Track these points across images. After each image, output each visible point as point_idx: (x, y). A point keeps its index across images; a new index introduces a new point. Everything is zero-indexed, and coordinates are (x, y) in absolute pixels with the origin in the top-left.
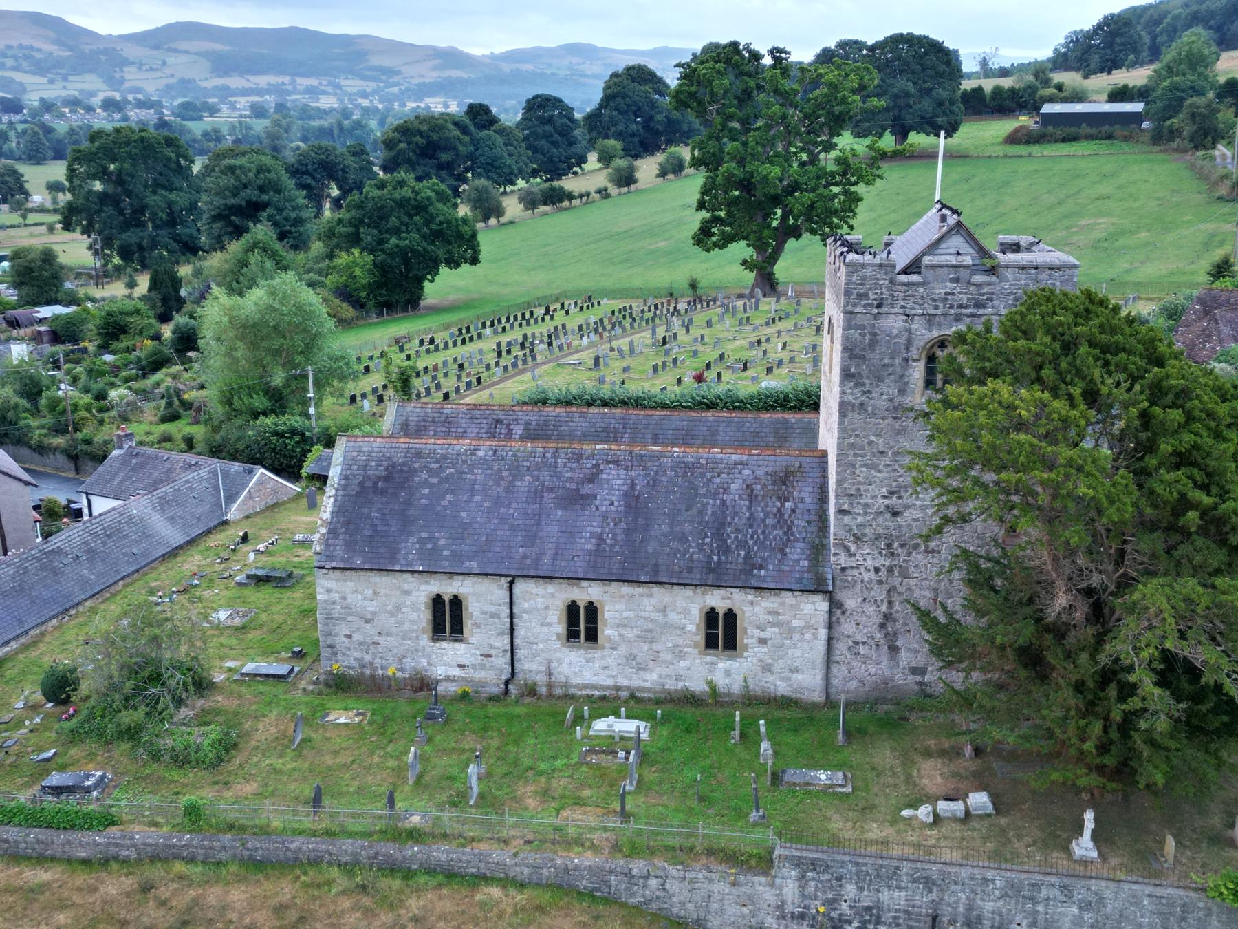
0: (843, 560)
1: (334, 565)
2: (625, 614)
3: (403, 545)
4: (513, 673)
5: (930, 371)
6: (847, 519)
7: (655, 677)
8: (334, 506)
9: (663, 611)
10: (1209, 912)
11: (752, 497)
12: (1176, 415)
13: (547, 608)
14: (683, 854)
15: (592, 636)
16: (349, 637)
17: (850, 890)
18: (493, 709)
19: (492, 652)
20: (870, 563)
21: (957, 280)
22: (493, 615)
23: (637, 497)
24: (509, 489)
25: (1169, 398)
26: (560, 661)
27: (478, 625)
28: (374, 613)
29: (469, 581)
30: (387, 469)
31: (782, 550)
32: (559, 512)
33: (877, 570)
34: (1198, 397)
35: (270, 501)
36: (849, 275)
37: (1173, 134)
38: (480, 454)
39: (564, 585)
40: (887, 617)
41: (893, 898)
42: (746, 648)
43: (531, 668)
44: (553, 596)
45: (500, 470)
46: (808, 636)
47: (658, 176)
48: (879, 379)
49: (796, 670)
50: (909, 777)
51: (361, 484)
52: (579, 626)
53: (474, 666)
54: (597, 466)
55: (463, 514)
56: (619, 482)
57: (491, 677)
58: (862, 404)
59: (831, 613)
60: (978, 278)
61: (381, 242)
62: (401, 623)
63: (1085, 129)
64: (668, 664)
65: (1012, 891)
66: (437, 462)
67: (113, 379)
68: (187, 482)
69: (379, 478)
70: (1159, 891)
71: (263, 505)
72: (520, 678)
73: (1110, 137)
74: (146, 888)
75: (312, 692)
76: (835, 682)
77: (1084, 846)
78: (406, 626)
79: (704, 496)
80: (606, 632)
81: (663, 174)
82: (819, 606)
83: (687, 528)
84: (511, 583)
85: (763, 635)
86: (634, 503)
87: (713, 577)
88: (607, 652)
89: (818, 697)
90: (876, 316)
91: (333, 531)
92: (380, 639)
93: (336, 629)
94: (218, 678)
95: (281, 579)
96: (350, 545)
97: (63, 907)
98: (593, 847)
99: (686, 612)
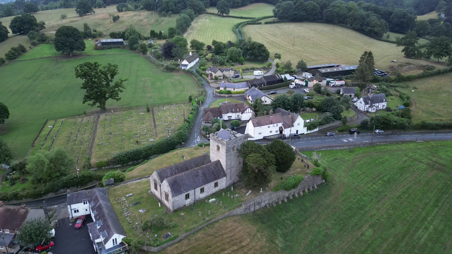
0: (227, 172)
9: (210, 185)
11: (215, 168)
14: (234, 208)
15: (203, 191)
17: (248, 204)
24: (189, 177)
37: (135, 49)
40: (231, 176)
41: (251, 203)
43: (197, 198)
49: (223, 186)
57: (193, 202)
60: (236, 139)
69: (173, 182)
72: (196, 200)
73: (119, 47)
74: (189, 240)
75: (173, 213)
80: (205, 190)
82: (225, 177)
86: (204, 174)
87: (216, 179)
89: (225, 188)
96: (175, 192)
97: (182, 246)
98: (227, 212)
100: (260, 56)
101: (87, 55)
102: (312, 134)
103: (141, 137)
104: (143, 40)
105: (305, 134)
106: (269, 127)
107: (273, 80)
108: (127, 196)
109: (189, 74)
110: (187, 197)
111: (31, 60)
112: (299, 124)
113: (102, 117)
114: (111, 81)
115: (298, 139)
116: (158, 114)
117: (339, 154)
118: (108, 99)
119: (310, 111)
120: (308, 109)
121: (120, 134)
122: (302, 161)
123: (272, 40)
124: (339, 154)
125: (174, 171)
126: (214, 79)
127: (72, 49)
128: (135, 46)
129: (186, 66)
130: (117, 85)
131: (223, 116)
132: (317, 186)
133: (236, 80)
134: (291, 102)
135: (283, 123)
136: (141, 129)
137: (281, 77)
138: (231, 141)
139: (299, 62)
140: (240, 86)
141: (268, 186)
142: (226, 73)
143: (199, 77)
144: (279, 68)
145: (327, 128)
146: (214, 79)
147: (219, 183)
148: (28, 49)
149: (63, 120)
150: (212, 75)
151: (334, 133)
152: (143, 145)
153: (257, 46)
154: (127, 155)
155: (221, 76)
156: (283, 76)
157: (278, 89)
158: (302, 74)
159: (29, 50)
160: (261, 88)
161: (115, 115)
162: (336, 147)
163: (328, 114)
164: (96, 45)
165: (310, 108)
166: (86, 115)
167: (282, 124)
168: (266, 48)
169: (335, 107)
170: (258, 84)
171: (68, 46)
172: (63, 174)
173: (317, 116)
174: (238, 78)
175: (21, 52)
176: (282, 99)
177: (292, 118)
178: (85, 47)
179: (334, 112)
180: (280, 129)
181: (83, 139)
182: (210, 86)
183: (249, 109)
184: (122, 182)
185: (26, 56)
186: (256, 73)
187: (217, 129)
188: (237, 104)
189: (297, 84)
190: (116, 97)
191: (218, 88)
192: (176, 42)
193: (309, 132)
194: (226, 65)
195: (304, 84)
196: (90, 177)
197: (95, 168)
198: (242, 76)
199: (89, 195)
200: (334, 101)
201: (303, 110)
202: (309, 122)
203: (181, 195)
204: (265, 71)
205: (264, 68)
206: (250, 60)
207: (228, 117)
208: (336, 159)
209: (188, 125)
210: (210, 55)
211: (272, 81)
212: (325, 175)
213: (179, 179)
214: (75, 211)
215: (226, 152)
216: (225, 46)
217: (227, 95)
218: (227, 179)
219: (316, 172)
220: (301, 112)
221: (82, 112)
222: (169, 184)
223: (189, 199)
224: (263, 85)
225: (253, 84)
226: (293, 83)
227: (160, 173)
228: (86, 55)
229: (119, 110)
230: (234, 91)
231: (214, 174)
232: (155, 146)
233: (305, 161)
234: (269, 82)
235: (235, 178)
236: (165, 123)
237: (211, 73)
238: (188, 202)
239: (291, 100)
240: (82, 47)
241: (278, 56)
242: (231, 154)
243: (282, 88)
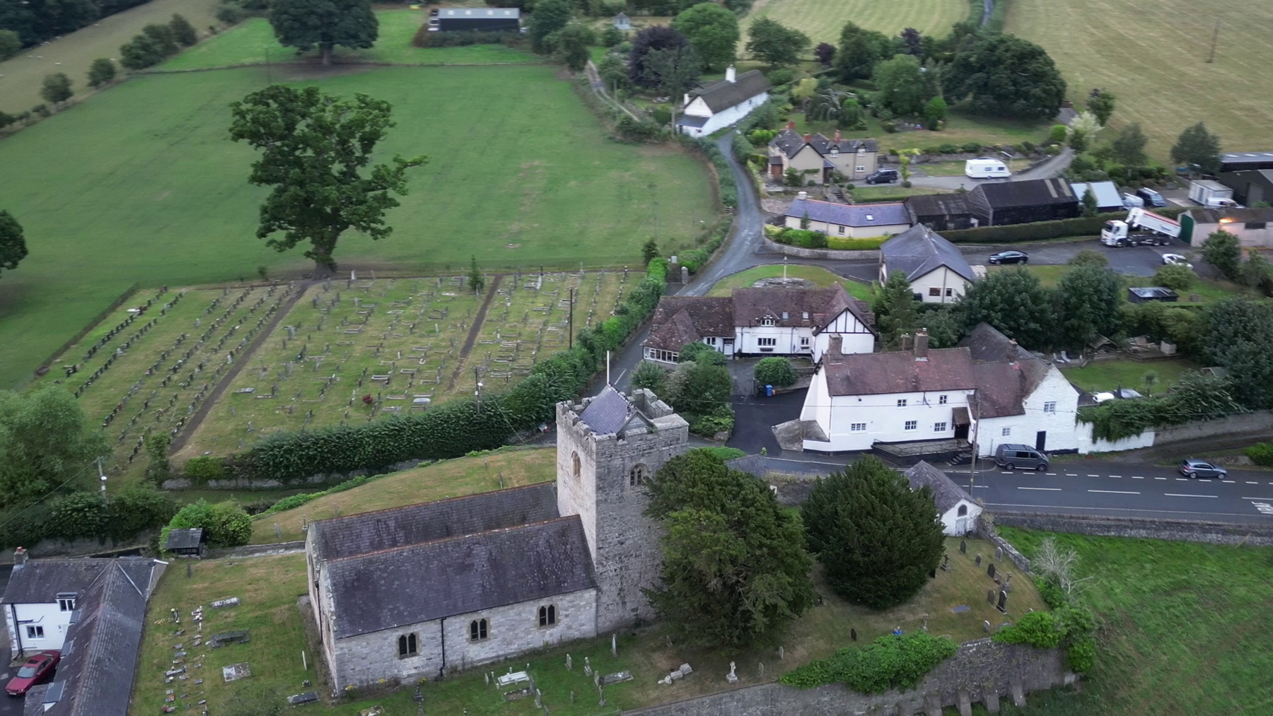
0: (601, 569)
1: (347, 635)
2: (501, 620)
3: (381, 615)
4: (444, 664)
5: (632, 478)
6: (601, 551)
7: (516, 646)
8: (334, 602)
9: (519, 614)
10: (780, 689)
11: (550, 546)
12: (752, 510)
13: (461, 627)
15: (484, 635)
18: (443, 686)
19: (432, 656)
20: (612, 568)
21: (641, 440)
22: (432, 638)
23: (495, 560)
25: (748, 503)
26: (468, 652)
27: (424, 645)
28: (367, 654)
29: (419, 625)
30: (356, 574)
31: (572, 571)
32: (458, 577)
33: (615, 570)
34: (758, 500)
36: (597, 446)
38: (405, 554)
39: (470, 614)
40: (621, 590)
42: (559, 621)
43: (454, 658)
44: (464, 621)
45: (419, 561)
46: (587, 608)
47: (90, 85)
48: (612, 487)
49: (583, 625)
50: (652, 664)
51: (344, 586)
52: (477, 631)
53: (422, 666)
54: (469, 547)
55: (408, 590)
56: (483, 553)
57: (432, 670)
58: (606, 500)
59: (597, 595)
60: (650, 437)
62: (383, 655)
63: (478, 34)
64: (522, 638)
65: (713, 704)
66: (383, 564)
69: (353, 580)
70: (763, 687)
72: (448, 665)
73: (498, 41)
75: (339, 703)
76: (599, 625)
77: (732, 677)
79: (528, 551)
80: (492, 631)
81: (95, 83)
82: (593, 593)
84: (442, 621)
85: (567, 613)
86: (495, 563)
87: (544, 592)
88: (492, 640)
89: (594, 634)
90: (609, 461)
95: (241, 638)
96: (351, 622)
100: (1018, 95)
101: (378, 61)
102: (1117, 459)
103: (394, 386)
104: (596, 16)
105: (1081, 455)
106: (902, 403)
107: (1027, 204)
108: (217, 603)
109: (698, 154)
110: (408, 646)
111: (198, 71)
112: (1050, 407)
113: (314, 291)
114: (362, 161)
115: (1037, 470)
116: (502, 301)
117: (1211, 567)
118: (347, 227)
119: (1145, 356)
120: (1138, 343)
121: (330, 364)
122: (991, 571)
123: (1121, 31)
124: (1211, 567)
125: (389, 534)
126: (785, 181)
127: (328, 41)
128: (551, 37)
129: (700, 121)
130: (382, 180)
131: (739, 335)
132: (1027, 695)
133: (876, 191)
134: (1045, 305)
135: (972, 392)
136: (413, 352)
137: (1068, 194)
138: (620, 442)
139: (1188, 131)
140: (870, 217)
141: (779, 658)
142: (839, 161)
143: (736, 174)
144: (1085, 153)
145: (1200, 438)
146: (785, 181)
147: (563, 613)
148: (202, 32)
149: (184, 290)
150: (781, 165)
151: (1220, 465)
152: (385, 413)
153: (1008, 54)
154: (301, 445)
155: (816, 171)
156: (1080, 189)
157: (1044, 243)
158: (1188, 187)
159: (206, 36)
160: (962, 231)
161: (358, 289)
162: (1205, 530)
163: (1215, 376)
164: (425, 27)
165: (1149, 341)
166: (267, 280)
167: (968, 396)
168: (1051, 63)
169: (1247, 346)
170: (952, 216)
171: (316, 28)
172: (56, 485)
173: (1156, 380)
174: (888, 182)
175: (178, 45)
176: (1004, 286)
177: (1022, 377)
178: (374, 36)
179: (1241, 370)
180: (954, 420)
181: (201, 367)
182: (760, 208)
183: (851, 318)
184: (238, 549)
185: (191, 58)
186: (978, 167)
187: (686, 385)
188: (804, 293)
189: (1139, 226)
190: (373, 225)
191: (780, 220)
192: (692, 28)
193: (1103, 446)
194: (864, 129)
195: (1173, 230)
196: (145, 511)
197: (182, 480)
198: (906, 177)
199: (87, 579)
200: (1250, 320)
201: (1110, 348)
202: (1106, 402)
203: (378, 635)
204: (1024, 164)
205: (1024, 148)
206: (974, 114)
207: (760, 340)
208: (1186, 586)
209: (582, 359)
210: (807, 85)
211: (1024, 208)
212: (1074, 651)
213: (384, 571)
214: (32, 632)
215: (599, 488)
216: (887, 50)
217: (806, 252)
218: (604, 599)
219: (1027, 632)
220: (1101, 356)
221: (254, 269)
222: (334, 585)
223: (415, 659)
224: (974, 221)
225: (926, 214)
226: (1118, 223)
227: (329, 536)
228: (375, 64)
230: (840, 236)
231: (541, 570)
232: (418, 424)
233: (1003, 571)
234: (1008, 210)
235: (638, 604)
236: (509, 338)
237: (779, 158)
238: (410, 668)
239: (1047, 297)
240: (365, 34)
241: (1102, 106)
242: (621, 498)
243: (1069, 239)
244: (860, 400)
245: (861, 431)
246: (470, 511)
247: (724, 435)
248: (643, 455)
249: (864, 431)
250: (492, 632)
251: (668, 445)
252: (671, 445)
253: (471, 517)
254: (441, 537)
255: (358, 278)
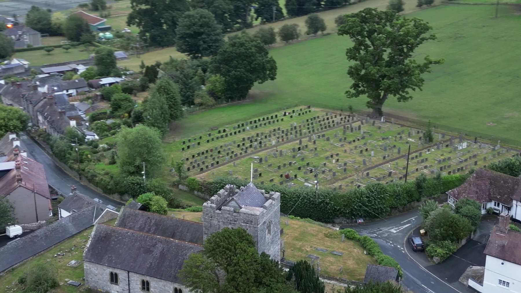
2: (156, 285)
8: (91, 243)
9: (164, 286)
16: (91, 279)
19: (125, 289)
21: (229, 214)
22: (125, 280)
29: (119, 270)
32: (143, 254)
35: (110, 218)
38: (129, 234)
51: (98, 238)
52: (145, 286)
54: (156, 242)
55: (120, 251)
56: (160, 248)
60: (235, 214)
61: (229, 71)
62: (103, 278)
67: (108, 133)
68: (84, 211)
69: (103, 237)
71: (107, 220)
78: (105, 279)
79: (180, 256)
83: (173, 264)
86: (163, 255)
91: (89, 250)
92: (99, 281)
93: (89, 276)
94: (61, 284)
99: (170, 288)
111: (476, 4)
131: (514, 206)
138: (218, 211)
197: (185, 186)
203: (102, 266)
213: (116, 238)
229: (409, 124)
244: (503, 264)
245: (505, 287)
246: (188, 229)
247: (436, 259)
248: (230, 224)
249: (507, 288)
250: (151, 289)
251: (245, 223)
252: (247, 223)
253: (187, 233)
254: (169, 237)
255: (386, 121)
